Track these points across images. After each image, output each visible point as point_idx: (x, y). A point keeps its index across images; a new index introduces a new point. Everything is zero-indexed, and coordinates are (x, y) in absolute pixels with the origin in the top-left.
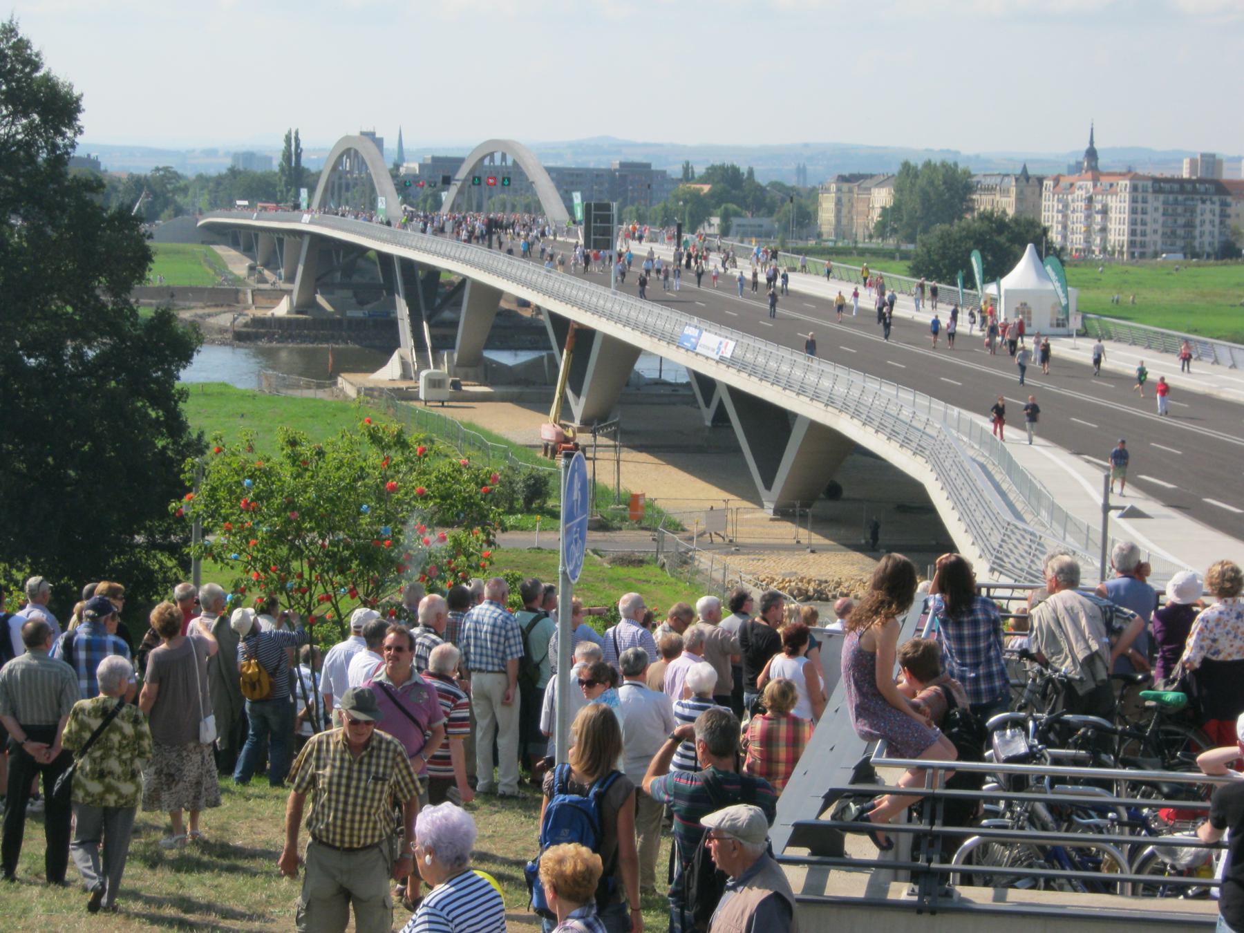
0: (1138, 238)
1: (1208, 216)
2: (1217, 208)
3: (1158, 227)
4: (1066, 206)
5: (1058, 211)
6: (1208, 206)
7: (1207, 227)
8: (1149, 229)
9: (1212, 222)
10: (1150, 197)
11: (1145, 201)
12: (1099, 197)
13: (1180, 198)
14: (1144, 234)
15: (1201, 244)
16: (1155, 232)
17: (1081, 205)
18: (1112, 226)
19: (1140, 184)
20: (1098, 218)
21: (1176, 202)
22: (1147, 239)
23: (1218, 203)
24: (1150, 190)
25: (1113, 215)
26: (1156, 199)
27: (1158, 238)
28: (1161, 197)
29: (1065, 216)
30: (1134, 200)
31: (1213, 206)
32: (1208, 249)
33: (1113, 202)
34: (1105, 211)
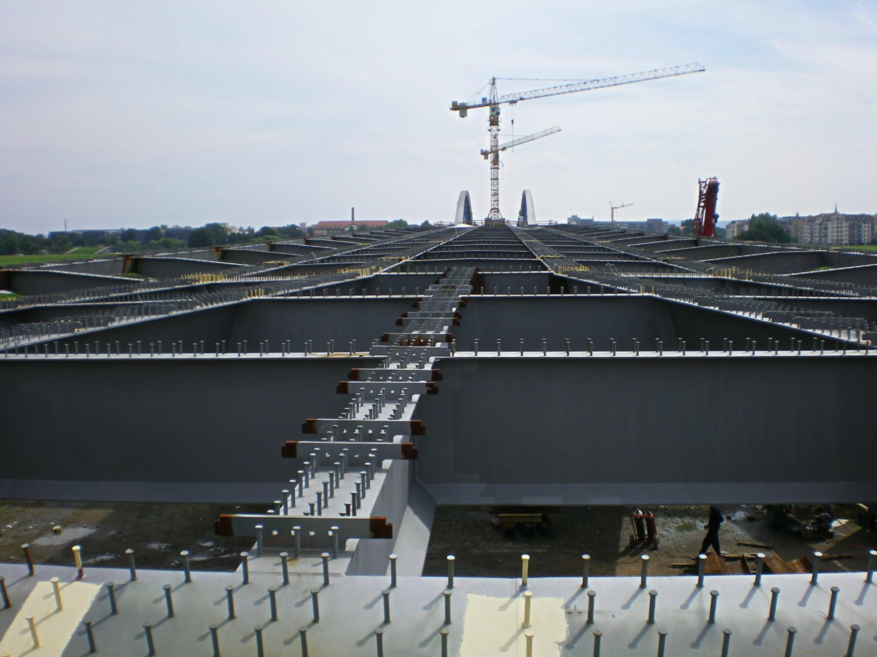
0: (840, 238)
1: (867, 229)
2: (870, 225)
3: (847, 233)
4: (812, 227)
5: (810, 229)
6: (867, 225)
7: (866, 233)
8: (844, 234)
9: (868, 231)
10: (844, 222)
11: (842, 224)
12: (825, 223)
13: (856, 222)
14: (842, 236)
15: (865, 240)
16: (846, 235)
17: (818, 226)
18: (830, 234)
19: (840, 217)
20: (825, 231)
21: (854, 224)
22: (843, 238)
23: (871, 224)
24: (844, 219)
25: (830, 230)
26: (846, 223)
27: (847, 237)
28: (848, 222)
29: (812, 231)
30: (838, 224)
31: (869, 225)
32: (866, 241)
33: (829, 225)
34: (826, 228)
